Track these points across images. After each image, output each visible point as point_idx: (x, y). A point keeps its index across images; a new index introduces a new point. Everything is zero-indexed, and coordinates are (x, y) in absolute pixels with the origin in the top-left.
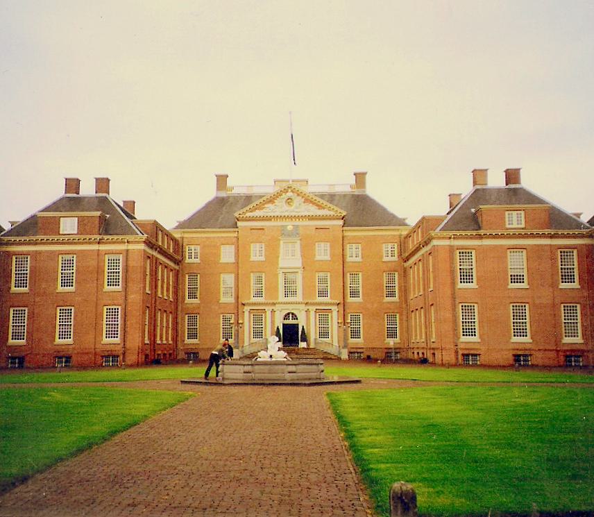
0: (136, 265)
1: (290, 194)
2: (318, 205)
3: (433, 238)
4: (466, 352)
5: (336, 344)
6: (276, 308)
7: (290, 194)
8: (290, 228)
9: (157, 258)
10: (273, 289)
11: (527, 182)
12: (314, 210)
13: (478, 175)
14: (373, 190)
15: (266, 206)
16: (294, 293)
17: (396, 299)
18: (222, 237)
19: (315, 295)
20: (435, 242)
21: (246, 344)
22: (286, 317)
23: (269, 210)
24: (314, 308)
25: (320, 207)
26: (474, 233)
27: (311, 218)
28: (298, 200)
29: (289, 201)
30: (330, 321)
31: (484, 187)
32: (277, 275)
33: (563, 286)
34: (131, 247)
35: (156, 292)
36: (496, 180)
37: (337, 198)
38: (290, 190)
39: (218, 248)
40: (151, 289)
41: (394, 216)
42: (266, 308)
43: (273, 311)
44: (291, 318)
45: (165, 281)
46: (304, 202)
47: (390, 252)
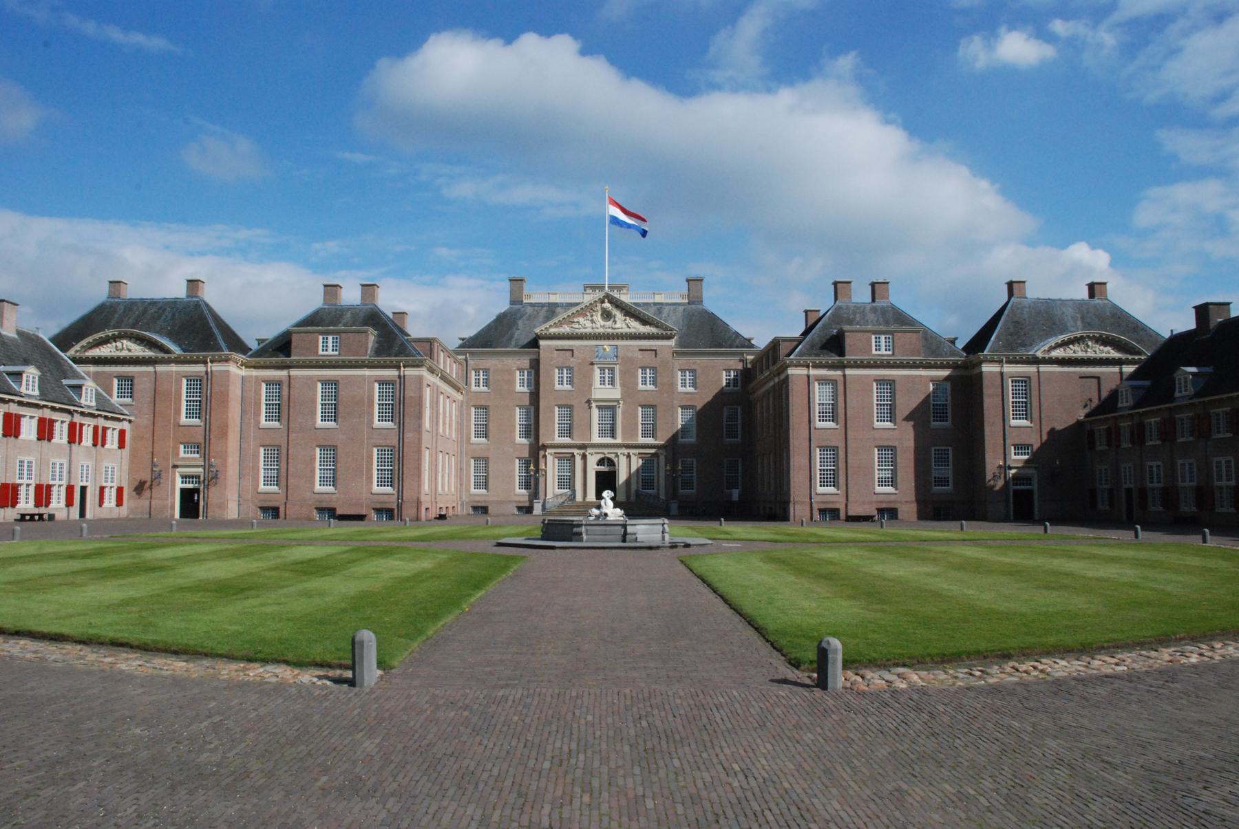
0: (413, 395)
1: (607, 305)
3: (788, 366)
4: (823, 506)
5: (662, 497)
6: (589, 451)
9: (438, 387)
11: (898, 298)
14: (713, 302)
15: (576, 320)
17: (739, 439)
19: (637, 436)
20: (791, 371)
21: (549, 496)
22: (600, 462)
23: (584, 325)
24: (637, 451)
25: (644, 321)
28: (618, 315)
30: (655, 468)
33: (935, 424)
35: (437, 430)
36: (861, 295)
37: (666, 310)
38: (606, 300)
39: (512, 373)
40: (431, 425)
42: (575, 451)
43: (584, 457)
44: (606, 464)
45: (447, 415)
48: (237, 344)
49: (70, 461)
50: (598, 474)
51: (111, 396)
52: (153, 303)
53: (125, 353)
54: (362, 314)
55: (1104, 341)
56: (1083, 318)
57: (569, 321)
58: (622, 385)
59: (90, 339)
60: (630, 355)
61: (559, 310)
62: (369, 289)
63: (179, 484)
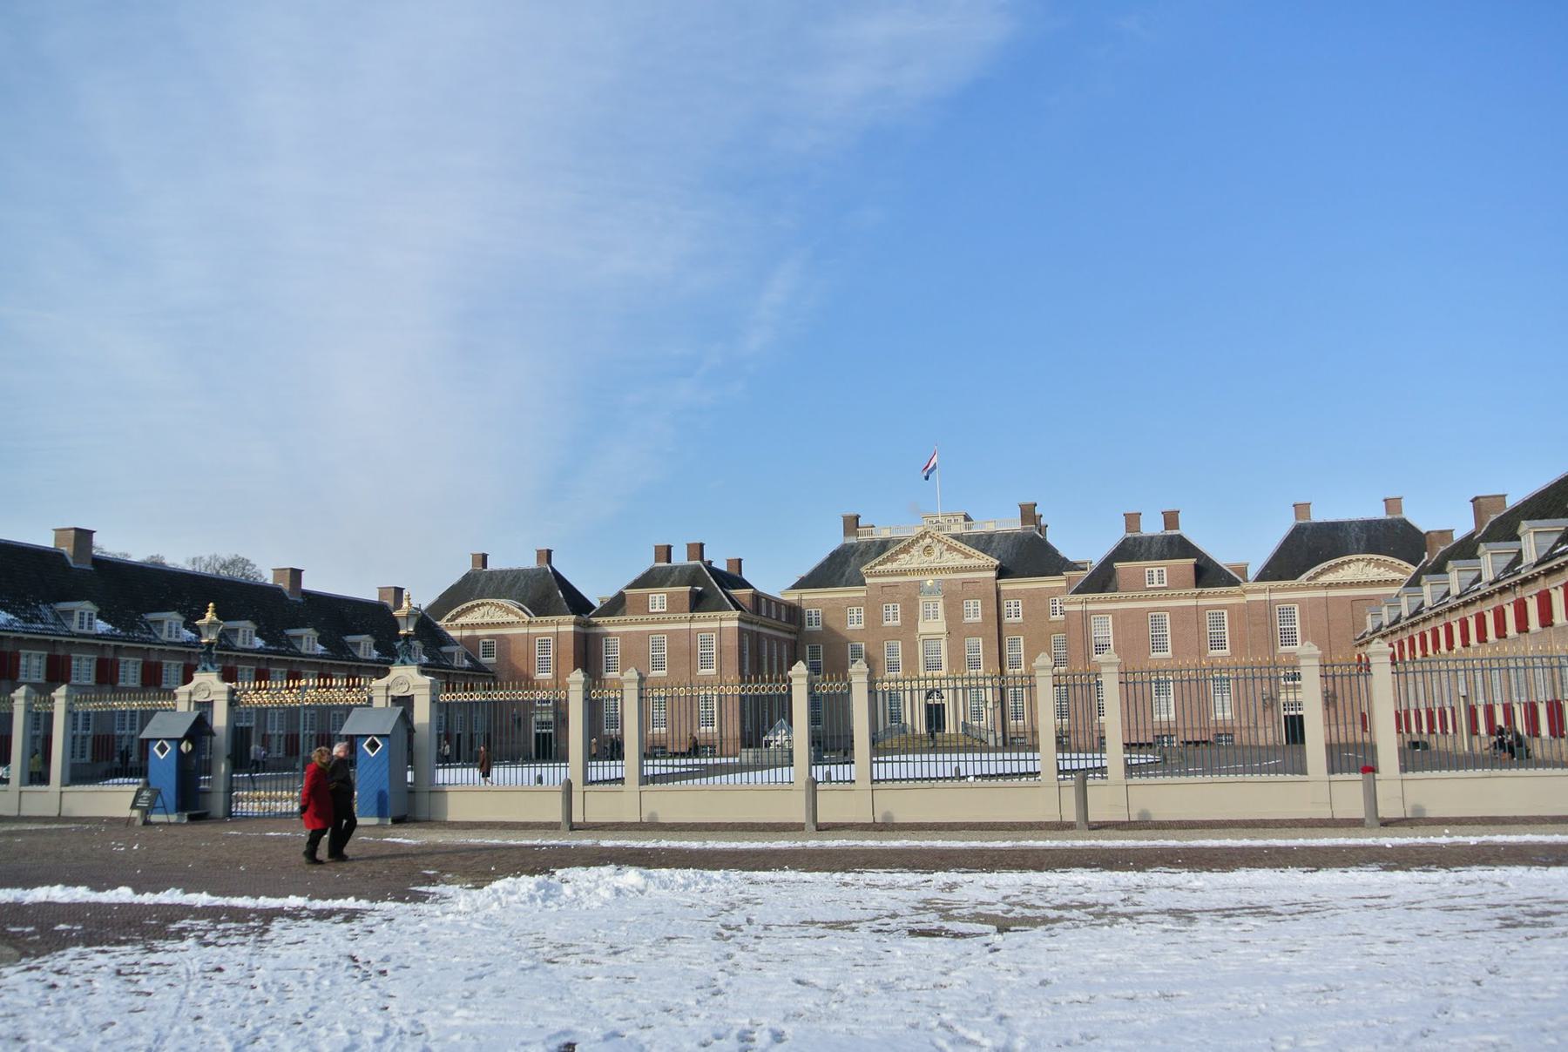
2: (963, 553)
7: (928, 540)
8: (929, 583)
9: (758, 633)
10: (911, 660)
12: (957, 560)
13: (1132, 520)
15: (900, 557)
16: (939, 667)
18: (848, 598)
25: (967, 556)
26: (1109, 595)
27: (956, 570)
29: (928, 550)
31: (1137, 535)
32: (915, 644)
34: (724, 624)
41: (1065, 560)
46: (947, 550)
47: (1058, 609)
48: (578, 604)
49: (447, 714)
50: (929, 707)
51: (478, 656)
52: (512, 571)
53: (487, 619)
54: (688, 572)
55: (1378, 564)
56: (1368, 540)
57: (891, 559)
58: (948, 618)
59: (459, 609)
60: (954, 588)
61: (890, 544)
62: (697, 550)
63: (535, 730)
